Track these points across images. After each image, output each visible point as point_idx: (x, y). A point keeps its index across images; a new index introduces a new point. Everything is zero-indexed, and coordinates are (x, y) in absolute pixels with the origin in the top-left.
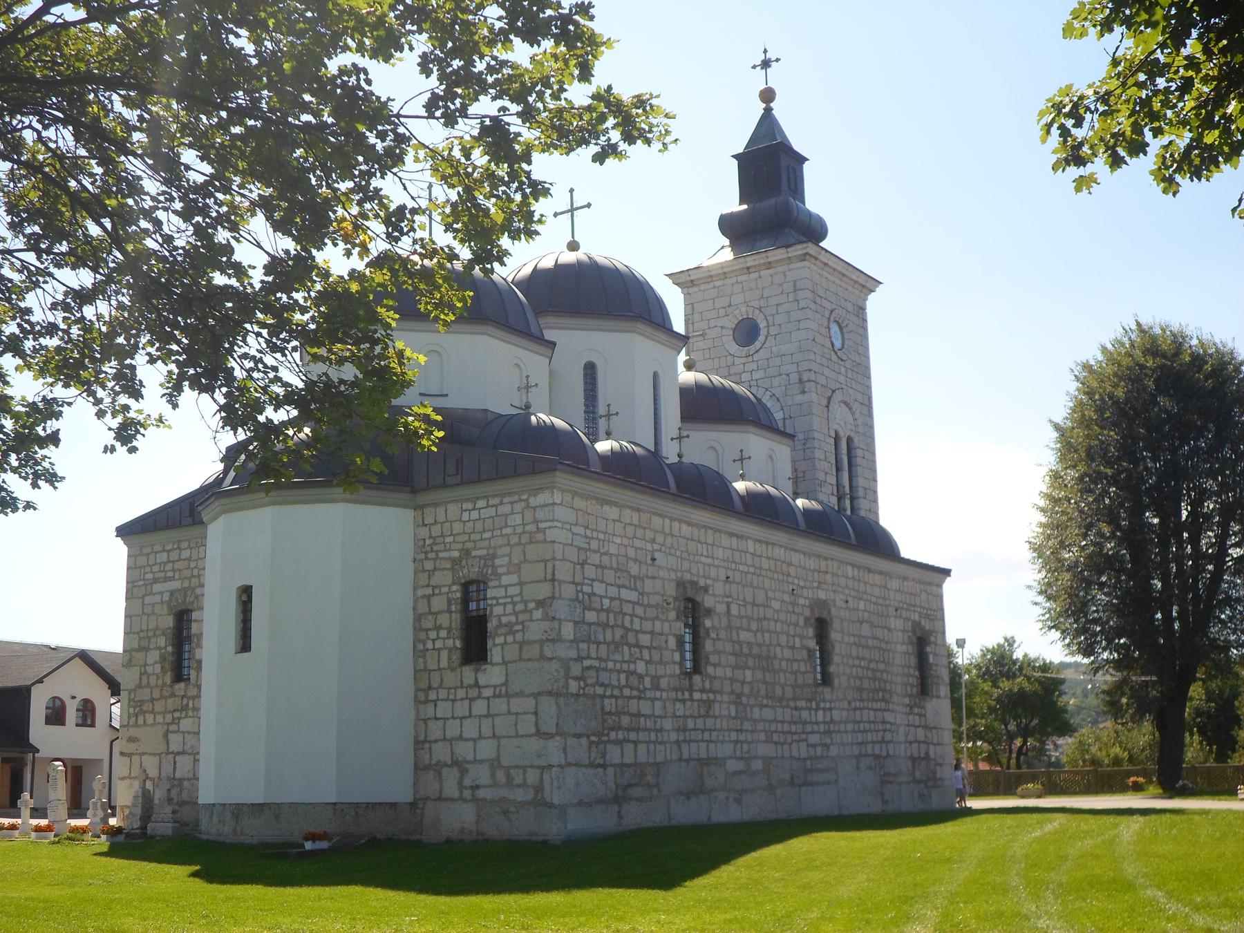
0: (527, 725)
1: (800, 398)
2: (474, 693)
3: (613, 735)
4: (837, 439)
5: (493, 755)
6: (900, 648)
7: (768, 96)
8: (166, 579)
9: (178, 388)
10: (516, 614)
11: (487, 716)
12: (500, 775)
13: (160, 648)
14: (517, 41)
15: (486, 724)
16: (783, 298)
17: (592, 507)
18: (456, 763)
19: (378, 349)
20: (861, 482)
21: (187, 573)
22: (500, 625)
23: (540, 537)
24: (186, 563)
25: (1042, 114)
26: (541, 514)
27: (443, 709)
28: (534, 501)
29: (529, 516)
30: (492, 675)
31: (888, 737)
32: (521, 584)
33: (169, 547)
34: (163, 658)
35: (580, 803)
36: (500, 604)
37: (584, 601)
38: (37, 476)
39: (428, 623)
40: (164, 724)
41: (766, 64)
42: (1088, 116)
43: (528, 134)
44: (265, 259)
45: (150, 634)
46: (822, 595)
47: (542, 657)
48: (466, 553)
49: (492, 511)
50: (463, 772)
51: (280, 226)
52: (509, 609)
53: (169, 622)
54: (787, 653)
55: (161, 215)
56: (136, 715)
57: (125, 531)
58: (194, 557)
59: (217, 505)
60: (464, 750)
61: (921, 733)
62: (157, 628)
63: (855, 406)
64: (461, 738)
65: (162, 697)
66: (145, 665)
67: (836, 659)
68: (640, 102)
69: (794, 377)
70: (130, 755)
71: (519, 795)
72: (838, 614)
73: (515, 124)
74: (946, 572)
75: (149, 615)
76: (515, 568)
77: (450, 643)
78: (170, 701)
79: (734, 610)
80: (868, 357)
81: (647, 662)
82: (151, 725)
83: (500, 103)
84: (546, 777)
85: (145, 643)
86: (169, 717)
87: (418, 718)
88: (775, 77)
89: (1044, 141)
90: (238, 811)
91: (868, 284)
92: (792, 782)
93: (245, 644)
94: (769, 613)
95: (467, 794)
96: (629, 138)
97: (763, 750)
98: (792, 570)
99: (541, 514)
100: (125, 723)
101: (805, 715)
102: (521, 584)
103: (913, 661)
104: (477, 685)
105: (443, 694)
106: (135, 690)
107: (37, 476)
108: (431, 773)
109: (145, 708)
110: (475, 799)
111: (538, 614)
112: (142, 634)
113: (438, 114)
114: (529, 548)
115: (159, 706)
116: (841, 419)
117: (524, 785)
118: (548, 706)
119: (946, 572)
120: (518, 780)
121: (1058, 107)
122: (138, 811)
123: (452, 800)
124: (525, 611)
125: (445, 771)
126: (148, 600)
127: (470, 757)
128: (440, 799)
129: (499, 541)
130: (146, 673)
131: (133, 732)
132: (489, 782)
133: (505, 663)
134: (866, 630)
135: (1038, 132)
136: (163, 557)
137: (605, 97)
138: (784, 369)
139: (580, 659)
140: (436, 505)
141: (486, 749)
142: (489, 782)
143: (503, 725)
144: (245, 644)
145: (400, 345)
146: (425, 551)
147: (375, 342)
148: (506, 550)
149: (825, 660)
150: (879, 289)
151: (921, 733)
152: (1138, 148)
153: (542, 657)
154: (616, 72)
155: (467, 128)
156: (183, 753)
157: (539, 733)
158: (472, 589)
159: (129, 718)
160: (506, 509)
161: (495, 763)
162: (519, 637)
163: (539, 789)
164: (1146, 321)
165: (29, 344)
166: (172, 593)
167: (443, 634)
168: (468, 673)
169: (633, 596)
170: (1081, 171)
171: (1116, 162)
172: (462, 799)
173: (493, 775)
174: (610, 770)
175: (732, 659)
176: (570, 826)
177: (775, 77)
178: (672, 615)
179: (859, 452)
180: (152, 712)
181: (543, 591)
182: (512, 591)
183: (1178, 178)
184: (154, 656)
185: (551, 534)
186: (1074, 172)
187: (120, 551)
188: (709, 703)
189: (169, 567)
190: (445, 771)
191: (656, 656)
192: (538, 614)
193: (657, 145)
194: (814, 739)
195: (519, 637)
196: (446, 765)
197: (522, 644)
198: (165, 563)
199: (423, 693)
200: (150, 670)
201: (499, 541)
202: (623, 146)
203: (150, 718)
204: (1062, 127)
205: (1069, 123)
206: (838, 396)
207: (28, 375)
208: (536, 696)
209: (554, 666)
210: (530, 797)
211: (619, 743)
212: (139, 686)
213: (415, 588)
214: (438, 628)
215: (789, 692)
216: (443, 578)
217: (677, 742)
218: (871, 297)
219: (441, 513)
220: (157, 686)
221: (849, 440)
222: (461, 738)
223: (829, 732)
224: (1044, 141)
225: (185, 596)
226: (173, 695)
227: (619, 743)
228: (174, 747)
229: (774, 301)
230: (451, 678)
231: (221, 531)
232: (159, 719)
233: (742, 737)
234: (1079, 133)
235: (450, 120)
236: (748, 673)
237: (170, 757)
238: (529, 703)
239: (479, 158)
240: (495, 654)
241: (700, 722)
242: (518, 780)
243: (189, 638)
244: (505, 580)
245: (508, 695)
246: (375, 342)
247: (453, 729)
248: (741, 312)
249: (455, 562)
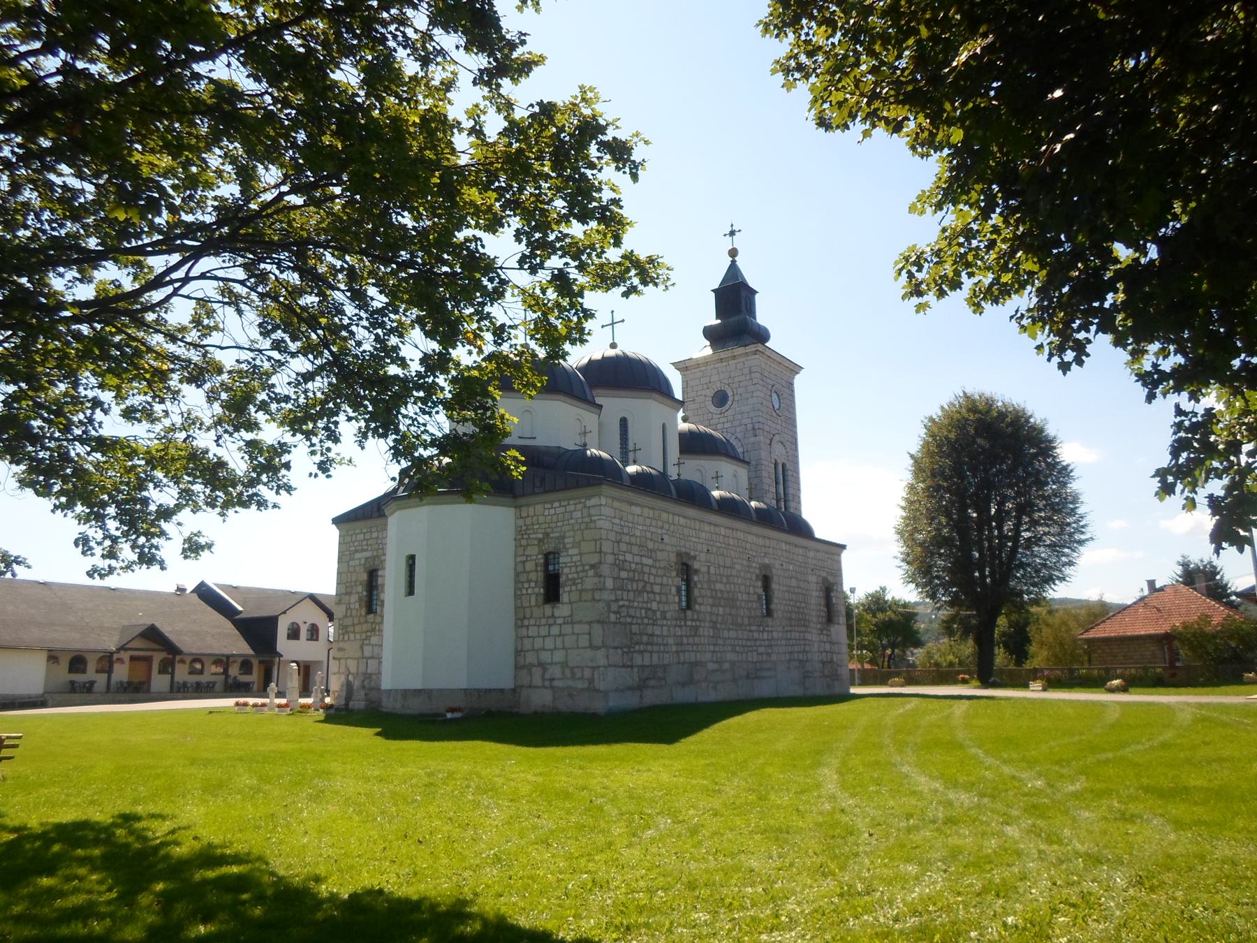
0: (584, 641)
1: (753, 439)
2: (551, 621)
3: (637, 647)
4: (776, 464)
6: (815, 594)
7: (733, 253)
8: (363, 550)
9: (365, 436)
10: (577, 573)
12: (568, 672)
14: (574, 222)
15: (559, 640)
16: (742, 378)
17: (624, 507)
19: (489, 413)
20: (790, 491)
22: (568, 579)
23: (592, 525)
25: (896, 263)
26: (593, 511)
27: (533, 631)
28: (589, 503)
29: (585, 514)
30: (563, 610)
31: (807, 648)
32: (580, 554)
34: (360, 599)
35: (617, 690)
36: (568, 566)
37: (619, 565)
38: (279, 487)
39: (523, 578)
41: (732, 233)
42: (926, 265)
43: (582, 279)
44: (421, 355)
46: (767, 561)
47: (594, 599)
48: (547, 535)
50: (545, 670)
51: (428, 334)
52: (573, 569)
53: (364, 577)
54: (745, 597)
55: (354, 328)
57: (337, 521)
59: (393, 505)
60: (545, 656)
61: (828, 647)
63: (787, 444)
64: (543, 649)
65: (359, 623)
67: (775, 601)
68: (651, 260)
69: (750, 427)
70: (339, 659)
71: (579, 685)
72: (776, 573)
73: (573, 273)
74: (843, 547)
76: (577, 545)
77: (537, 590)
78: (365, 627)
79: (712, 571)
80: (794, 414)
81: (659, 603)
83: (564, 260)
84: (596, 676)
86: (364, 636)
87: (517, 636)
88: (738, 241)
89: (896, 280)
90: (406, 693)
91: (795, 369)
92: (748, 677)
93: (411, 591)
94: (734, 573)
95: (547, 683)
96: (644, 282)
97: (731, 656)
98: (748, 546)
99: (593, 511)
101: (756, 635)
102: (580, 554)
103: (823, 602)
104: (553, 615)
105: (532, 622)
107: (279, 487)
108: (525, 671)
110: (552, 687)
111: (591, 573)
113: (526, 266)
114: (586, 532)
115: (358, 628)
116: (778, 451)
117: (582, 678)
118: (597, 629)
119: (843, 547)
120: (579, 675)
121: (907, 259)
122: (344, 694)
124: (583, 571)
125: (534, 669)
126: (352, 563)
128: (530, 686)
129: (567, 528)
131: (341, 645)
133: (570, 603)
134: (794, 583)
135: (893, 274)
137: (629, 257)
138: (744, 421)
139: (617, 600)
140: (528, 505)
141: (559, 656)
143: (569, 641)
144: (411, 591)
145: (502, 411)
146: (521, 534)
147: (487, 409)
148: (571, 533)
149: (768, 601)
150: (802, 372)
151: (828, 647)
152: (956, 285)
153: (594, 599)
154: (636, 241)
155: (544, 276)
157: (591, 647)
158: (550, 558)
160: (572, 508)
161: (564, 665)
162: (579, 587)
163: (591, 681)
164: (969, 391)
165: (274, 406)
166: (366, 559)
167: (533, 584)
168: (548, 609)
169: (650, 562)
170: (921, 300)
171: (941, 294)
172: (544, 687)
174: (636, 669)
175: (711, 601)
176: (611, 704)
177: (738, 241)
178: (674, 574)
179: (790, 473)
181: (594, 559)
182: (575, 559)
183: (983, 303)
184: (354, 598)
185: (600, 524)
186: (915, 300)
187: (334, 532)
188: (697, 628)
190: (534, 669)
191: (664, 599)
192: (591, 573)
193: (661, 287)
194: (761, 650)
195: (579, 587)
197: (581, 591)
199: (521, 620)
201: (567, 528)
202: (640, 287)
203: (352, 636)
204: (909, 272)
205: (914, 269)
206: (777, 438)
207: (274, 425)
208: (590, 623)
209: (601, 605)
210: (586, 685)
211: (641, 652)
213: (516, 556)
214: (529, 581)
215: (746, 621)
216: (533, 551)
217: (677, 652)
218: (797, 377)
219: (531, 510)
221: (784, 465)
223: (771, 646)
224: (896, 280)
226: (366, 622)
227: (641, 652)
229: (737, 379)
230: (537, 612)
231: (397, 521)
232: (358, 636)
233: (717, 649)
234: (920, 276)
235: (533, 270)
236: (721, 609)
238: (586, 628)
239: (552, 294)
240: (565, 597)
241: (691, 640)
242: (579, 675)
243: (377, 587)
244: (571, 552)
245: (572, 623)
246: (487, 409)
247: (538, 643)
249: (540, 540)
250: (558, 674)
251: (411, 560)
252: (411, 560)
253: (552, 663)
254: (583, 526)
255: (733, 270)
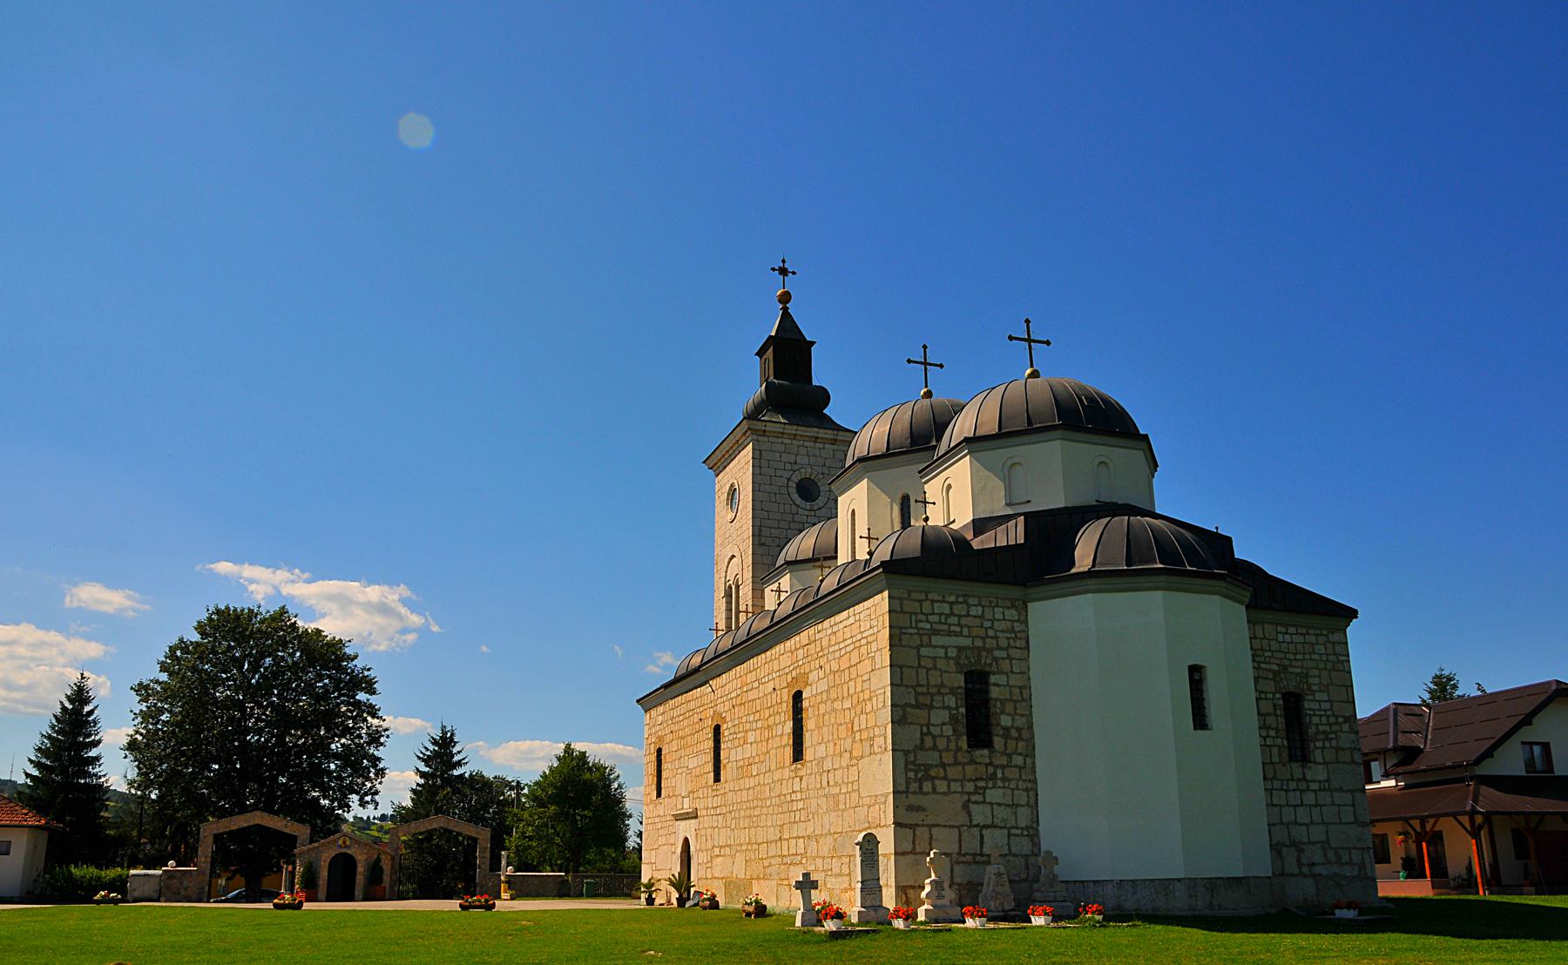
2: (1303, 785)
5: (1324, 837)
7: (785, 298)
8: (949, 634)
10: (1330, 725)
11: (1316, 806)
12: (1331, 854)
13: (948, 708)
15: (1316, 811)
18: (1293, 844)
21: (981, 632)
22: (1318, 732)
24: (978, 621)
30: (1317, 773)
33: (952, 599)
34: (954, 720)
40: (962, 793)
45: (932, 690)
49: (1301, 638)
50: (1300, 851)
56: (920, 781)
58: (988, 615)
62: (942, 685)
64: (1296, 823)
65: (956, 763)
66: (928, 725)
70: (913, 827)
71: (1348, 871)
75: (929, 670)
78: (969, 769)
82: (944, 794)
85: (926, 700)
86: (970, 786)
90: (1212, 884)
93: (1200, 720)
95: (1305, 870)
100: (903, 788)
104: (1304, 779)
105: (1277, 784)
106: (914, 751)
109: (933, 773)
110: (1314, 875)
111: (1346, 727)
112: (919, 689)
114: (1334, 674)
115: (953, 772)
117: (1350, 863)
120: (1346, 859)
123: (1293, 875)
125: (1284, 850)
126: (924, 651)
127: (1305, 839)
129: (1310, 664)
130: (929, 733)
132: (1322, 860)
136: (946, 609)
141: (1317, 833)
142: (1322, 860)
156: (993, 826)
157: (1357, 822)
159: (908, 784)
161: (1325, 845)
162: (1334, 743)
166: (960, 649)
168: (1297, 770)
172: (1301, 874)
173: (1325, 855)
180: (945, 778)
189: (954, 620)
190: (1284, 850)
192: (1346, 727)
195: (1334, 743)
196: (1284, 845)
198: (947, 616)
200: (935, 731)
201: (1310, 664)
203: (942, 786)
212: (922, 747)
220: (948, 750)
222: (1296, 823)
225: (979, 656)
226: (973, 762)
228: (978, 819)
232: (955, 787)
237: (976, 831)
244: (1318, 696)
245: (1330, 790)
248: (806, 472)
250: (1318, 856)
251: (1196, 674)
252: (1196, 674)
253: (1310, 843)
254: (1329, 666)
255: (786, 314)
